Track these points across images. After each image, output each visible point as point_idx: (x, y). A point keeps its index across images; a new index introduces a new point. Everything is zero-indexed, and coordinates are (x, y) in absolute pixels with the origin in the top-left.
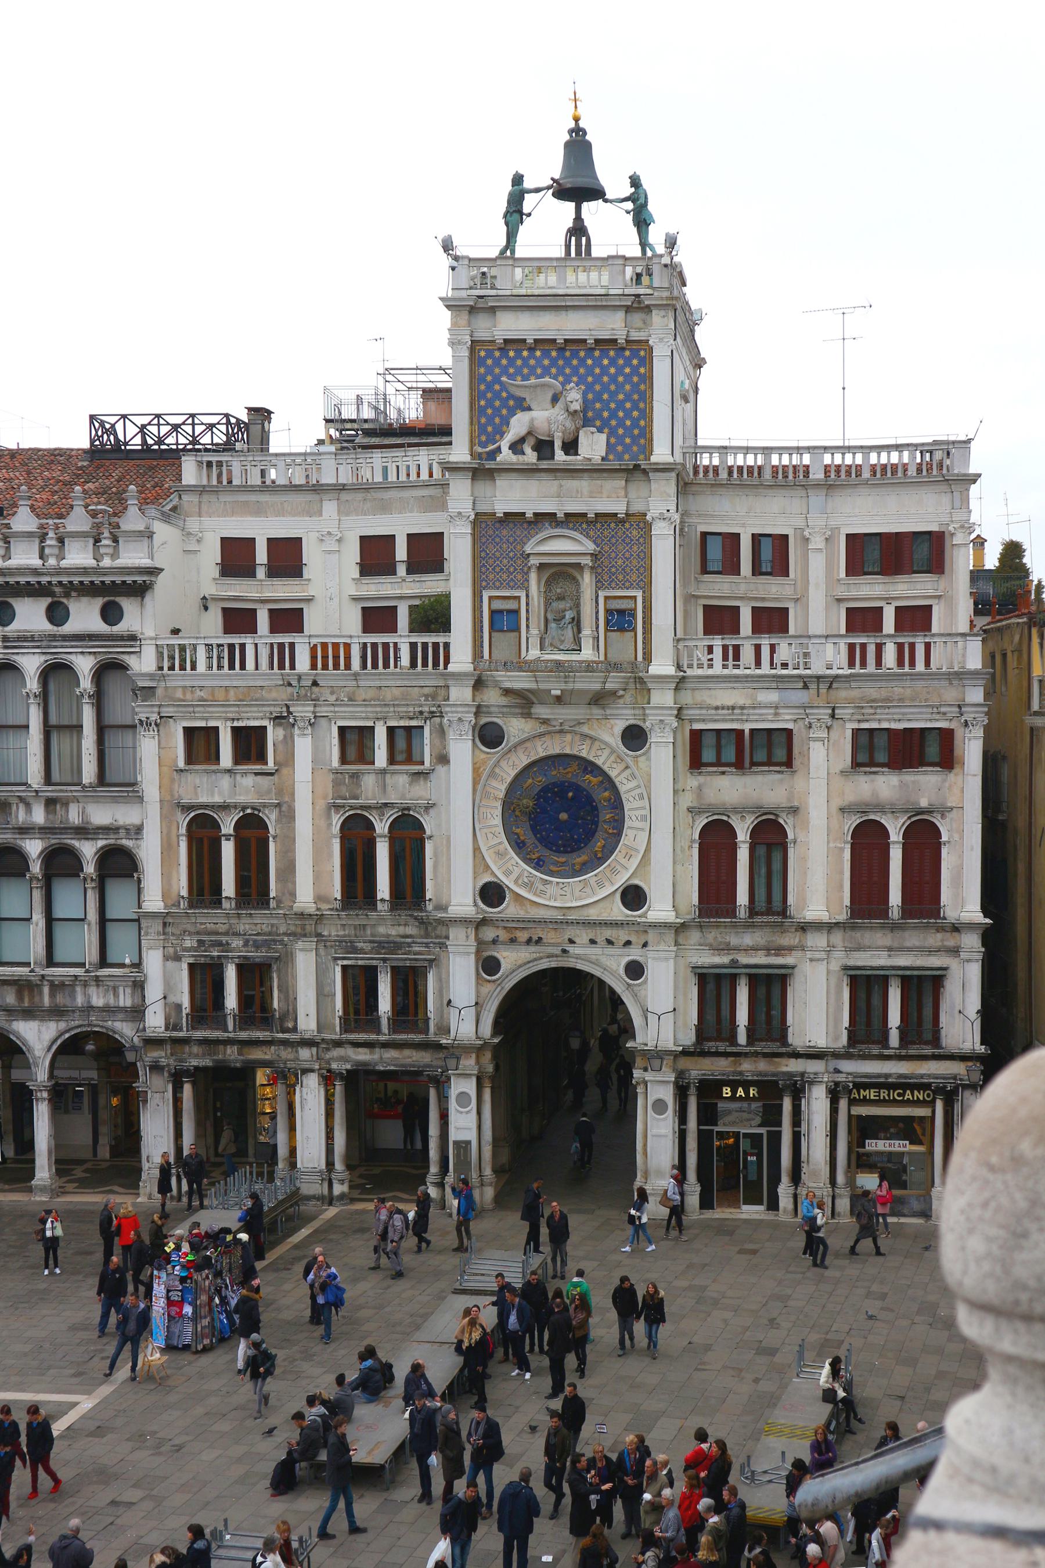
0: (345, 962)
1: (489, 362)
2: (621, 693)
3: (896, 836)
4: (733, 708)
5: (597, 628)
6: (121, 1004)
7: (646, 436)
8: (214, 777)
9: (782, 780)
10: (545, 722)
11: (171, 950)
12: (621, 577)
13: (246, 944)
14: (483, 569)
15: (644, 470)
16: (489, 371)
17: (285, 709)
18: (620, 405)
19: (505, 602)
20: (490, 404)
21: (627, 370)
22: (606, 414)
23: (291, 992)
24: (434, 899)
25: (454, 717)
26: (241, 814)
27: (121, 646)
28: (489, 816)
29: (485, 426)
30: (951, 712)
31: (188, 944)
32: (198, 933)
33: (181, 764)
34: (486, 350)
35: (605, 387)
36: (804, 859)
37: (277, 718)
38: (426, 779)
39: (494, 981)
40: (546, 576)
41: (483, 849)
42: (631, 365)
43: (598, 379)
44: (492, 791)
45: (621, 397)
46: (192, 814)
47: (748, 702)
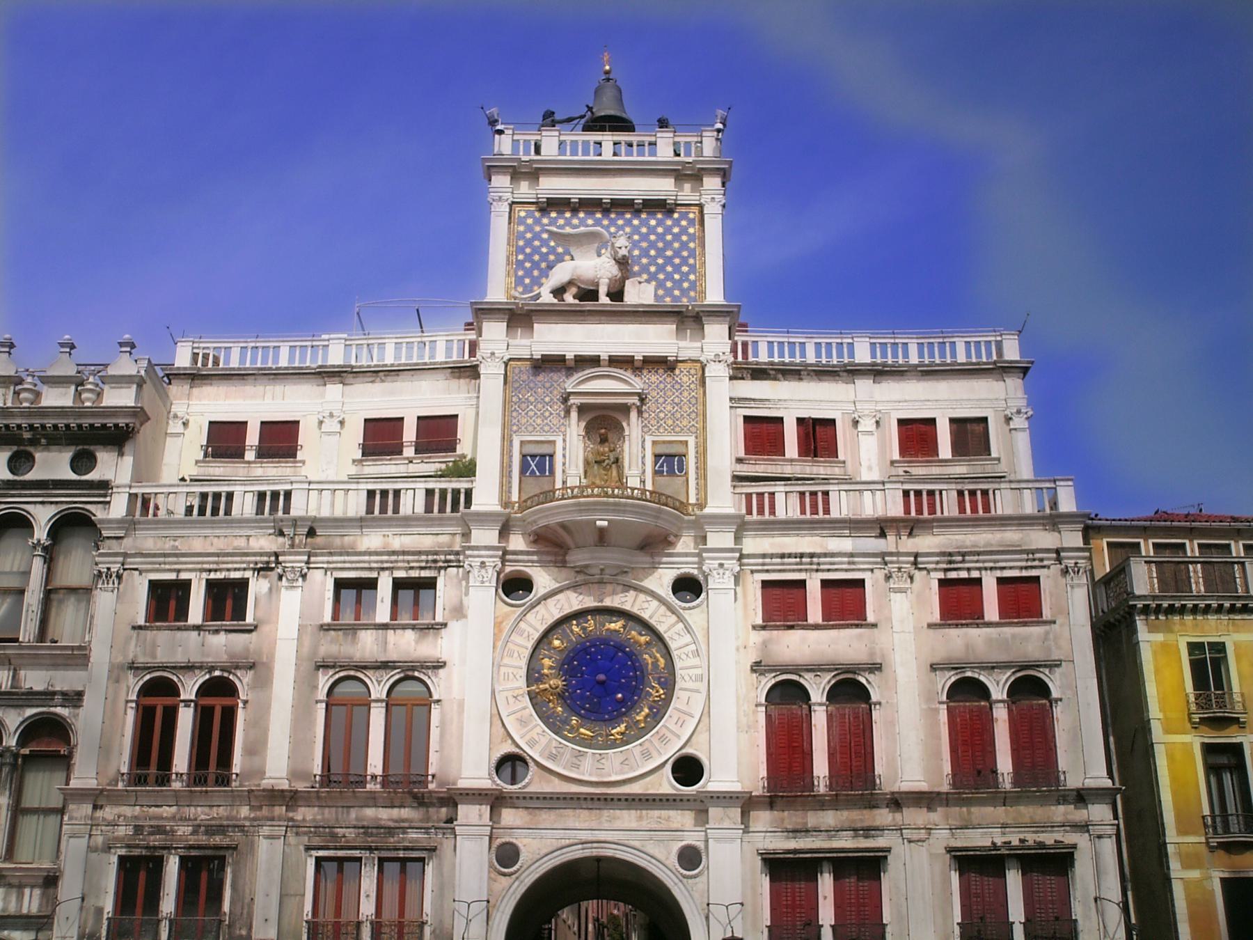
0: (321, 853)
1: (530, 221)
2: (672, 538)
4: (802, 556)
5: (644, 472)
6: (25, 911)
7: (698, 287)
8: (179, 634)
9: (860, 635)
10: (581, 570)
11: (99, 840)
12: (670, 422)
13: (195, 832)
14: (514, 414)
17: (273, 559)
18: (669, 260)
20: (529, 257)
21: (676, 230)
22: (653, 269)
23: (247, 891)
25: (476, 562)
26: (207, 677)
27: (84, 496)
29: (522, 278)
30: (1049, 559)
31: (122, 831)
32: (136, 818)
33: (141, 622)
35: (652, 245)
36: (891, 724)
37: (259, 570)
38: (436, 636)
39: (510, 875)
40: (589, 416)
42: (679, 226)
43: (644, 237)
44: (516, 648)
45: (669, 253)
46: (148, 677)
47: (818, 550)
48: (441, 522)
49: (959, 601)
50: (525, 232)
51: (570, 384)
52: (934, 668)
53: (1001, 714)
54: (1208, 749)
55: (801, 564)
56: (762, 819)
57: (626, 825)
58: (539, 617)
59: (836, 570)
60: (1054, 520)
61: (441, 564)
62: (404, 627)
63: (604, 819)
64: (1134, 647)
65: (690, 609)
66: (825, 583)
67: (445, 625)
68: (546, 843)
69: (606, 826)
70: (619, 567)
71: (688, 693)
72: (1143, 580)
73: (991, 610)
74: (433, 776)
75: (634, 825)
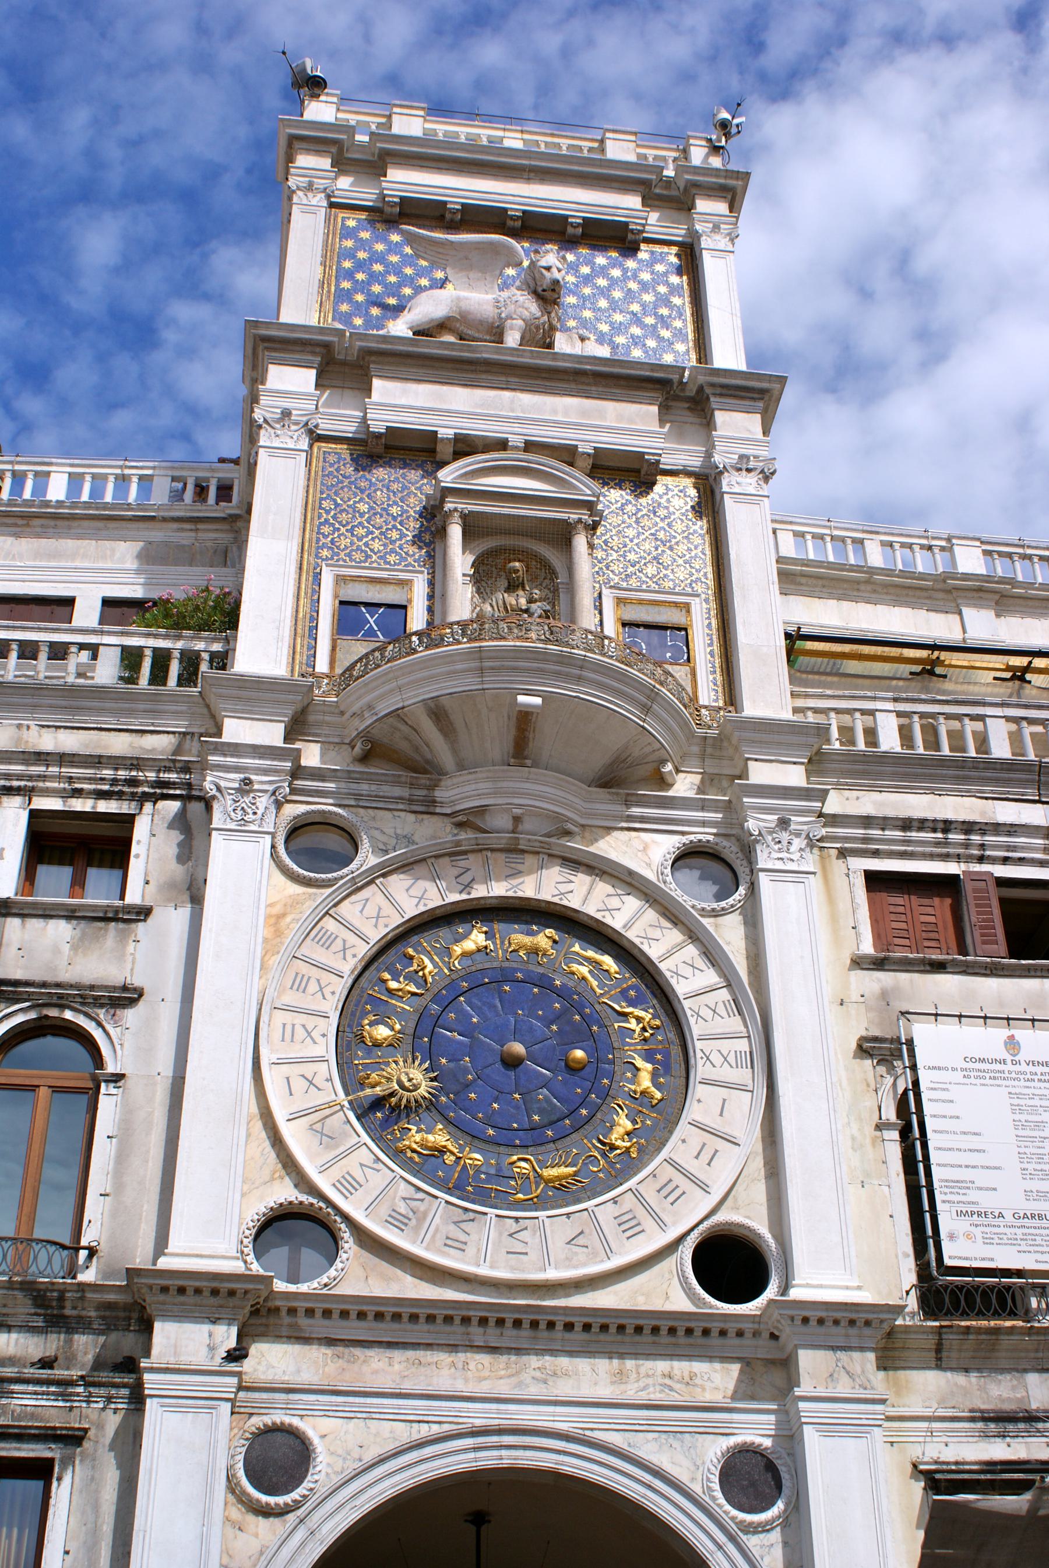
4: (947, 826)
10: (466, 820)
14: (326, 530)
15: (701, 389)
16: (362, 244)
19: (378, 586)
24: (103, 1249)
28: (300, 1033)
34: (358, 220)
41: (280, 1116)
44: (315, 972)
48: (154, 705)
50: (356, 249)
51: (448, 475)
55: (946, 843)
56: (927, 1387)
57: (587, 1392)
58: (371, 910)
59: (1021, 861)
61: (146, 789)
62: (47, 913)
63: (526, 1377)
65: (715, 914)
67: (144, 913)
68: (378, 1434)
69: (534, 1391)
70: (557, 817)
71: (723, 1092)
74: (92, 1252)
75: (605, 1391)
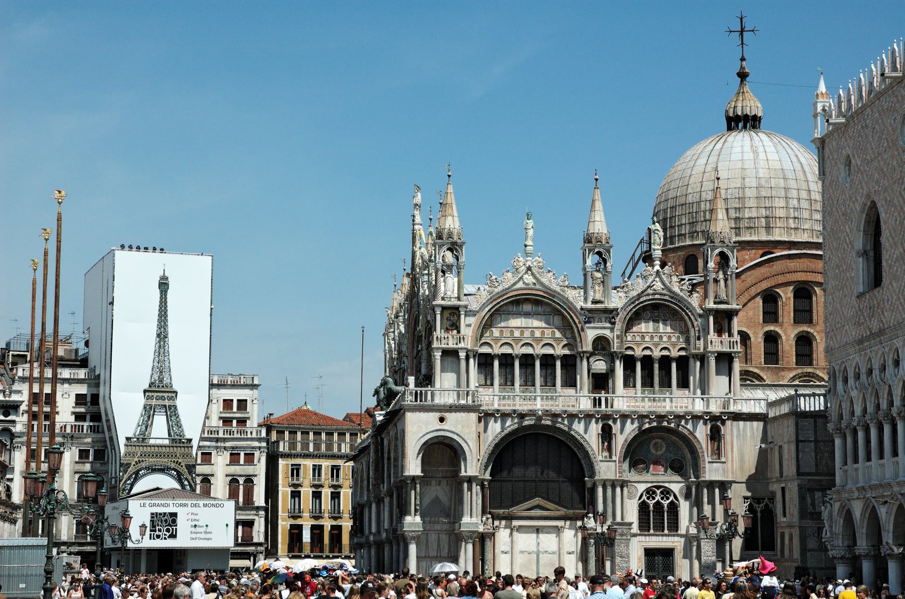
3: (241, 482)
36: (216, 489)
49: (234, 459)
52: (227, 476)
53: (241, 487)
54: (292, 492)
60: (260, 440)
64: (278, 464)
66: (202, 454)
72: (283, 447)
73: (242, 462)
